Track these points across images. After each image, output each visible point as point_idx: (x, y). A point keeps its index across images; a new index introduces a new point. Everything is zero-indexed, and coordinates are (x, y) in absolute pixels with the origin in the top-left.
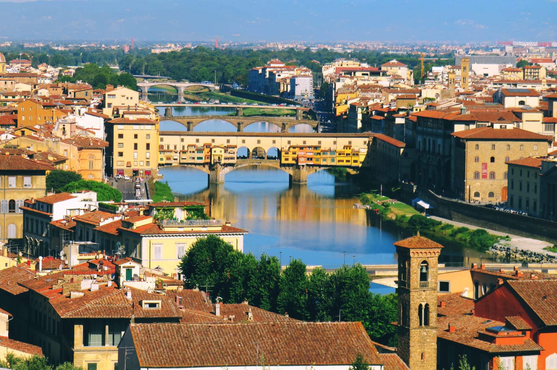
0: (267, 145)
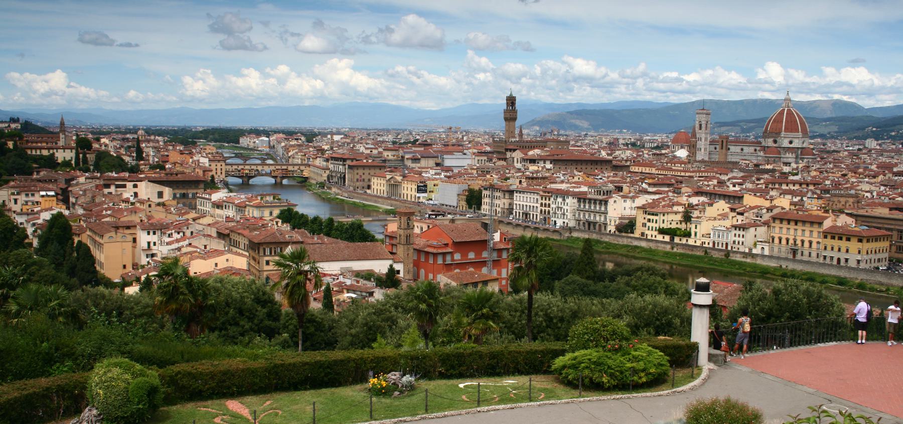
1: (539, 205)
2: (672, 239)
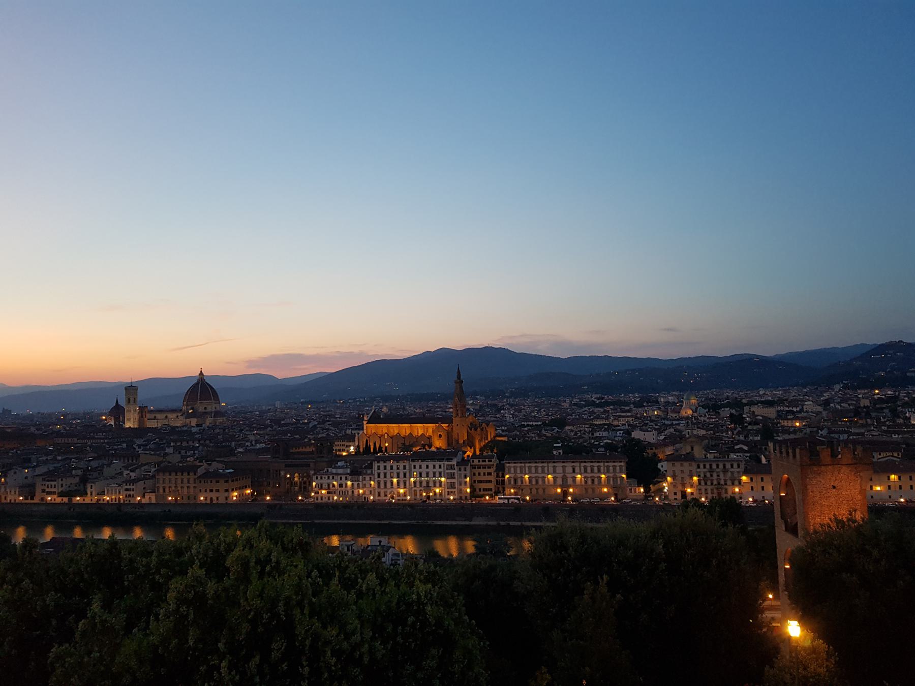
2: (70, 500)
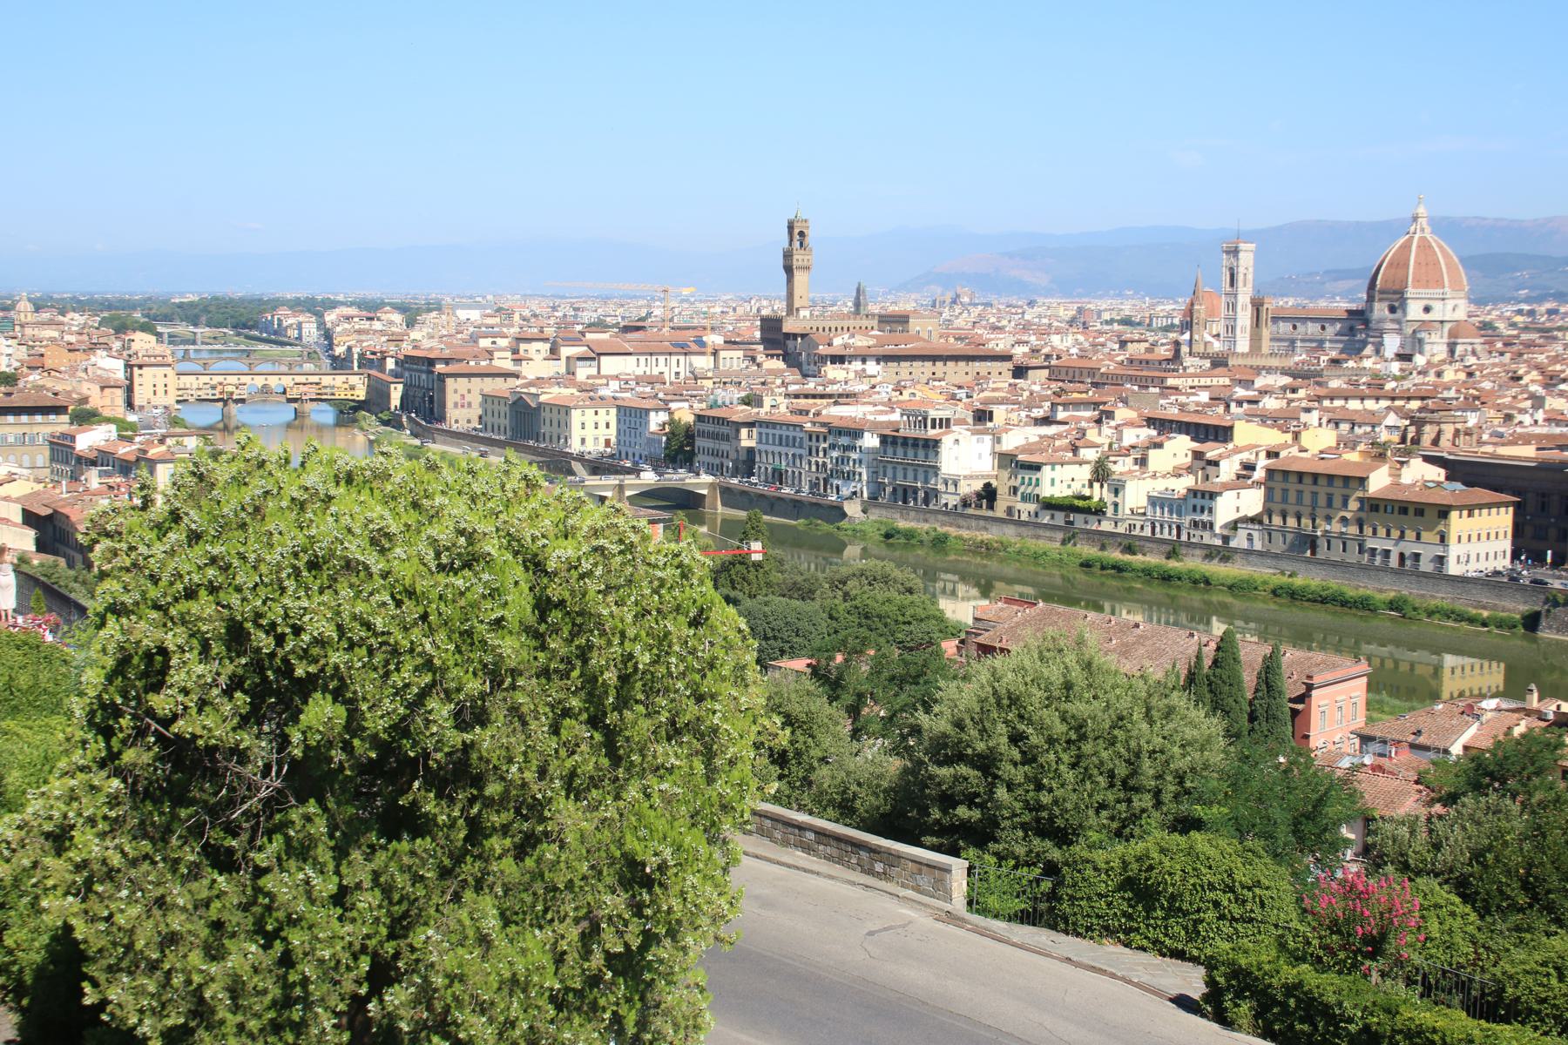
0: (273, 382)
1: (804, 452)
